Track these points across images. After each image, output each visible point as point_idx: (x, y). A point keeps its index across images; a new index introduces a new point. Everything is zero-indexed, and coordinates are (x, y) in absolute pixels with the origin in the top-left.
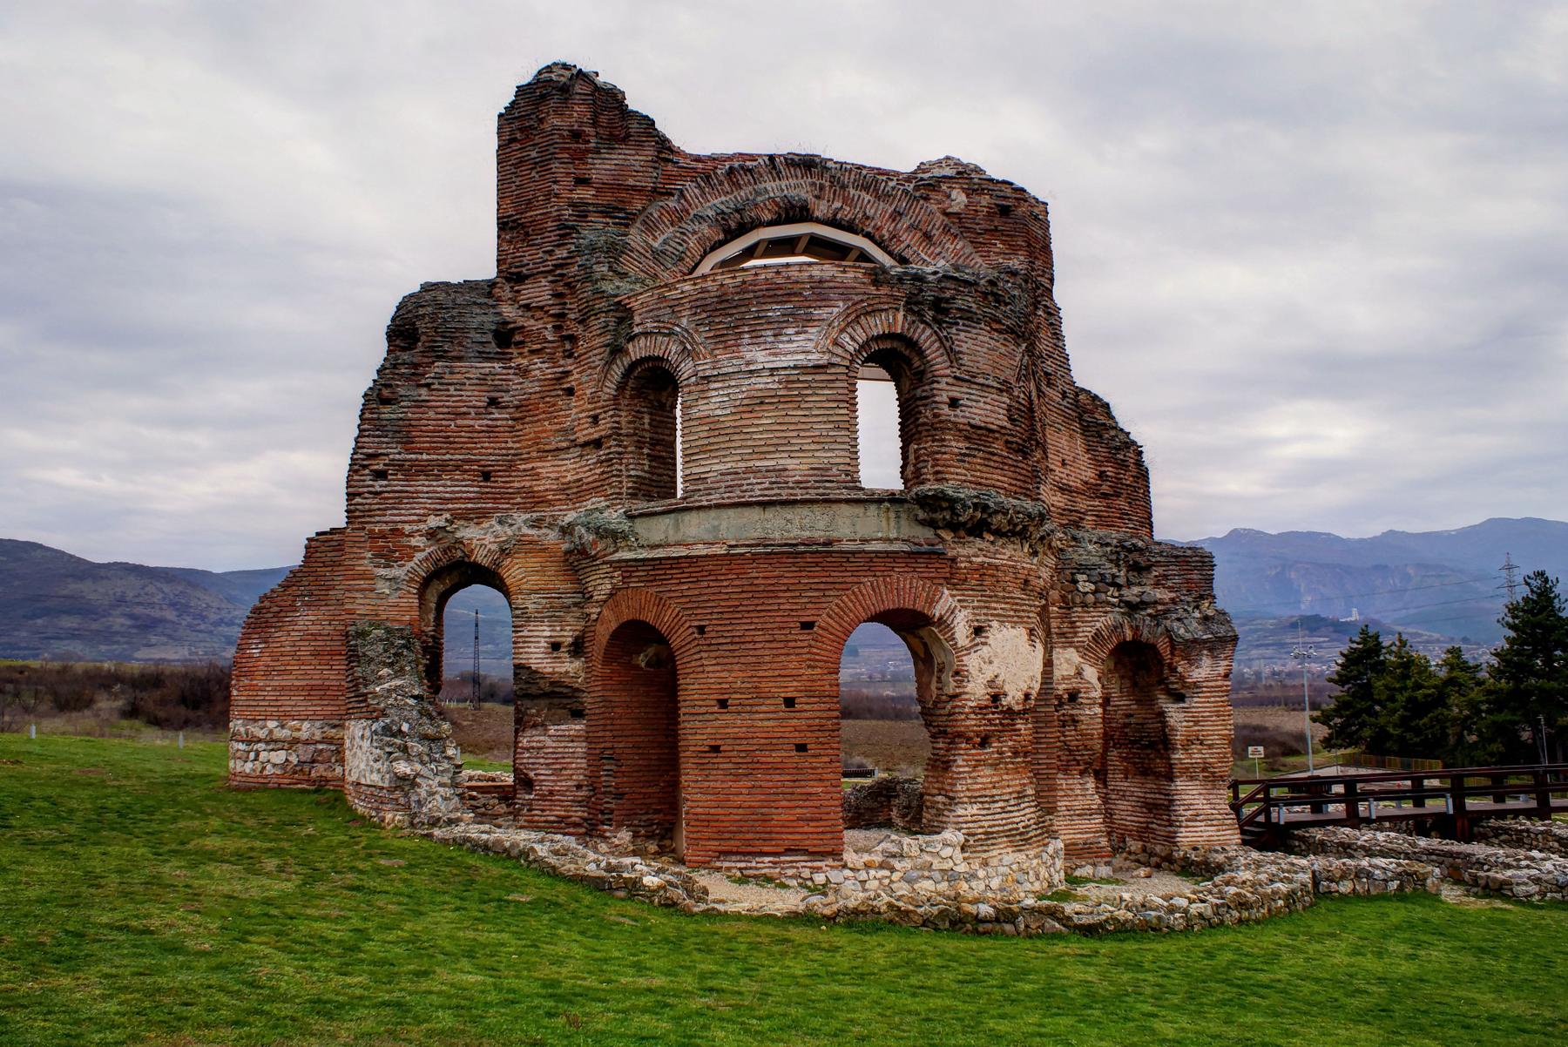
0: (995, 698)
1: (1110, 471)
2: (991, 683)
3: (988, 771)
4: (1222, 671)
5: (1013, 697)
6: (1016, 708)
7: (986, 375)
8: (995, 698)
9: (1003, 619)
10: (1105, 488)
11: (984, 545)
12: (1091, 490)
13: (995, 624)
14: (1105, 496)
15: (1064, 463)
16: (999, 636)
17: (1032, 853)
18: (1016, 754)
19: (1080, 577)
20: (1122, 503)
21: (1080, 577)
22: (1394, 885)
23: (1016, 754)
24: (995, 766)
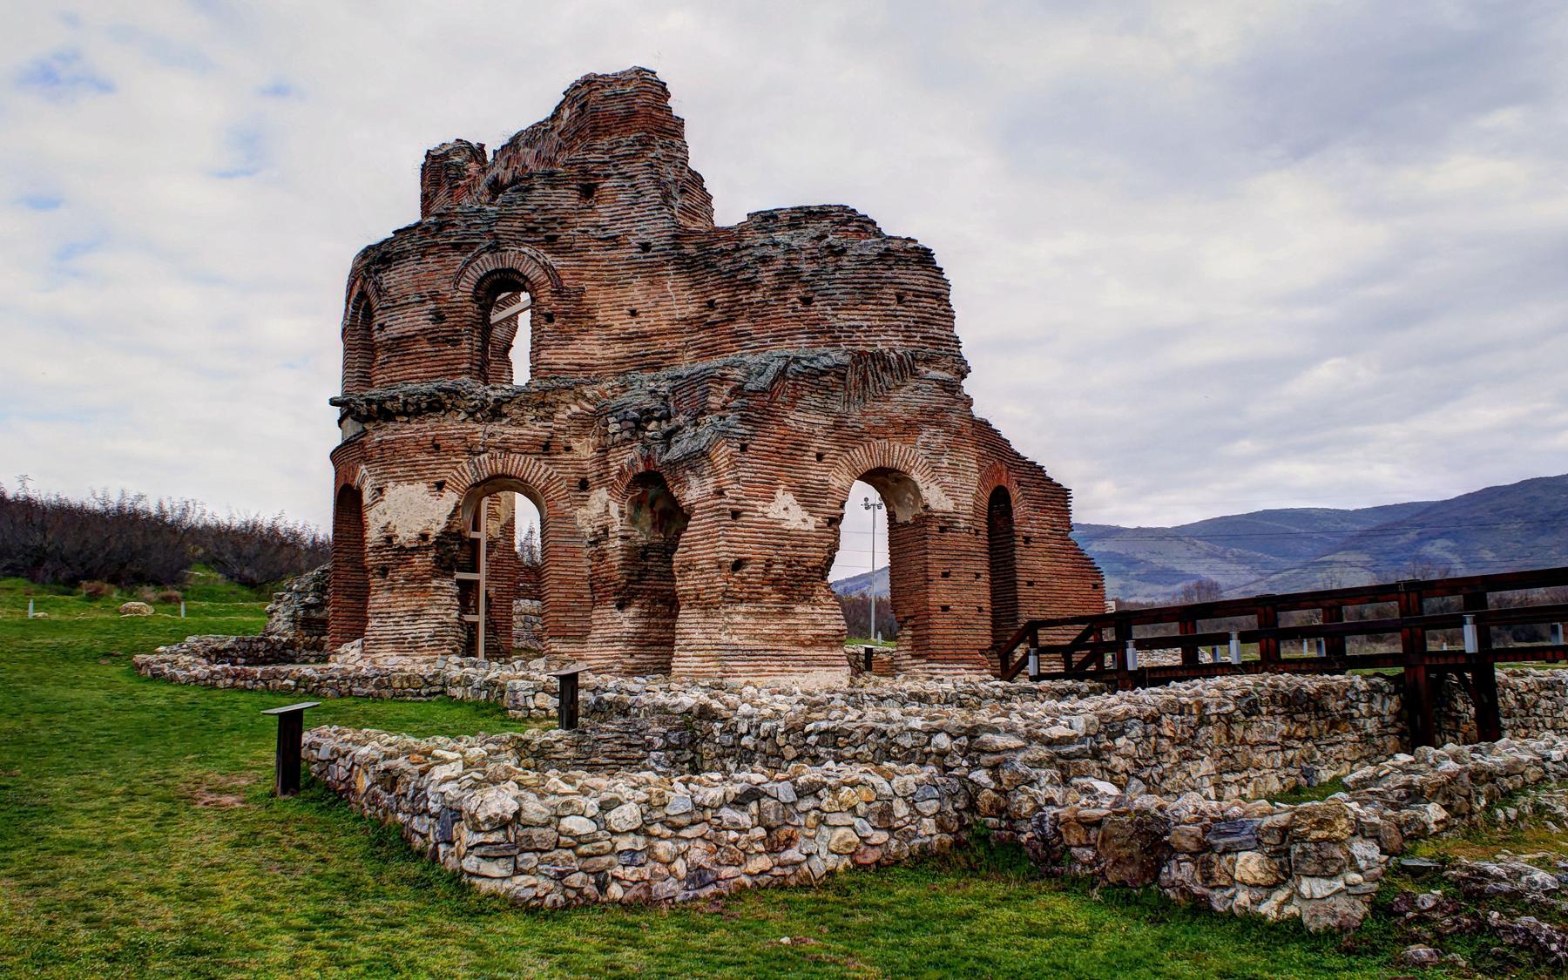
0: (389, 539)
1: (720, 297)
2: (385, 528)
3: (386, 594)
4: (710, 489)
5: (406, 534)
6: (408, 546)
7: (405, 296)
8: (389, 539)
9: (398, 480)
10: (714, 316)
11: (398, 426)
12: (699, 323)
13: (391, 484)
14: (713, 324)
15: (634, 313)
16: (393, 493)
17: (420, 659)
18: (408, 581)
19: (611, 420)
20: (742, 325)
21: (611, 420)
22: (483, 695)
23: (408, 581)
24: (391, 589)
